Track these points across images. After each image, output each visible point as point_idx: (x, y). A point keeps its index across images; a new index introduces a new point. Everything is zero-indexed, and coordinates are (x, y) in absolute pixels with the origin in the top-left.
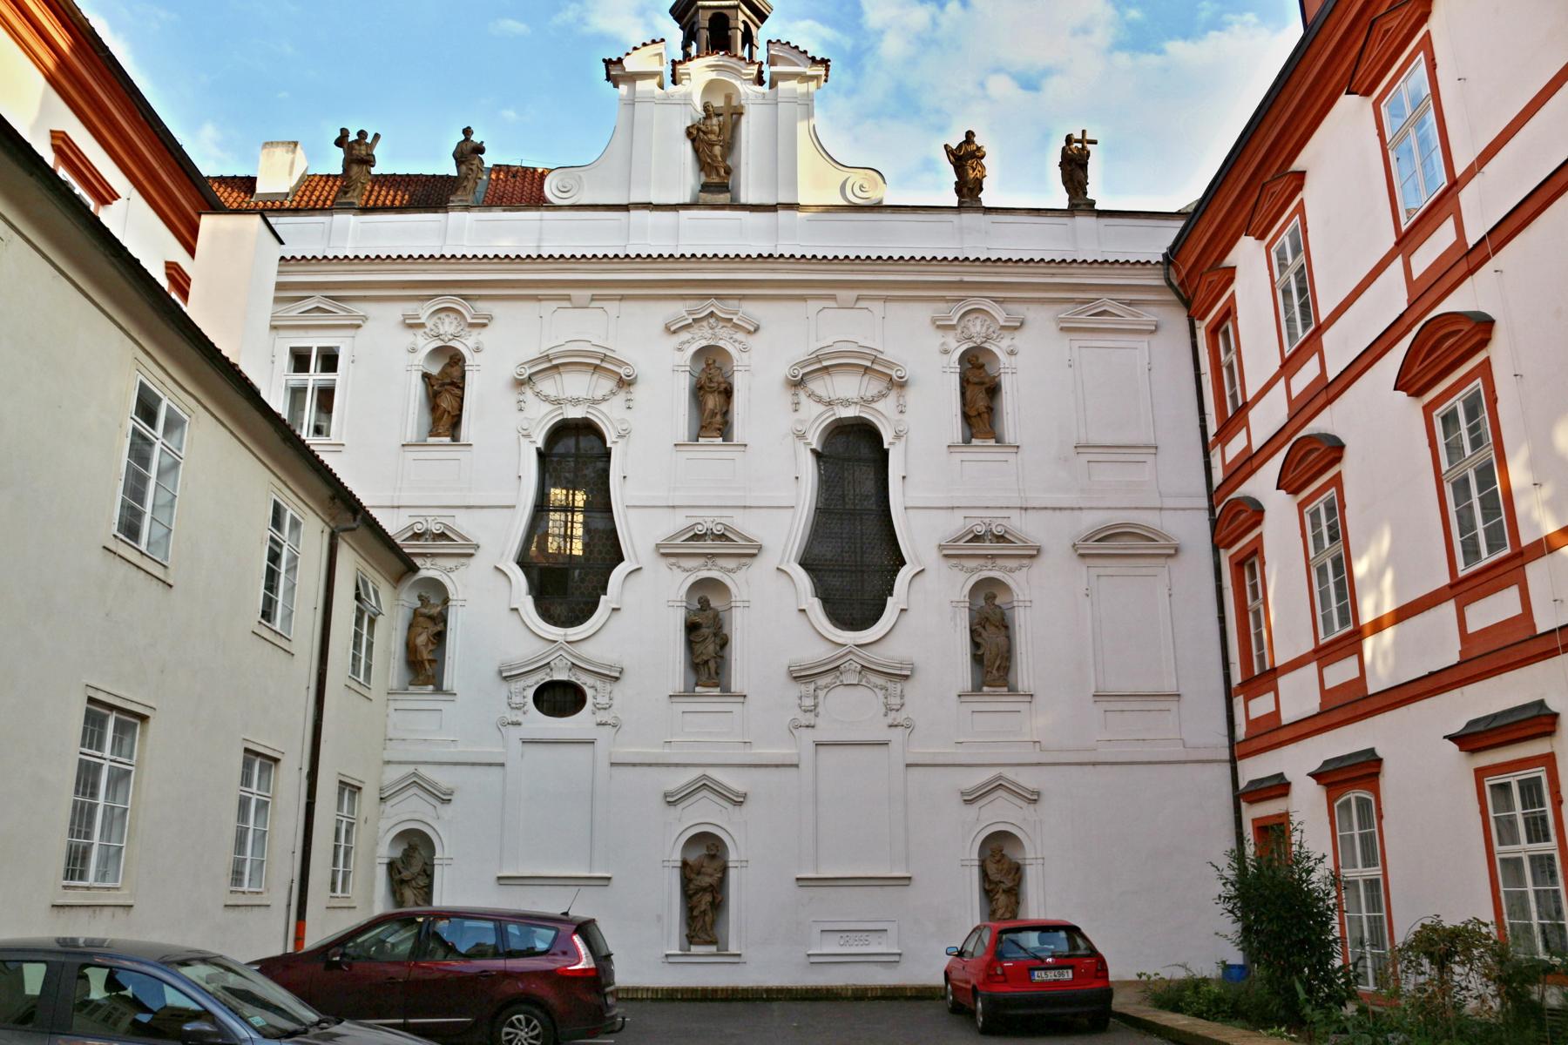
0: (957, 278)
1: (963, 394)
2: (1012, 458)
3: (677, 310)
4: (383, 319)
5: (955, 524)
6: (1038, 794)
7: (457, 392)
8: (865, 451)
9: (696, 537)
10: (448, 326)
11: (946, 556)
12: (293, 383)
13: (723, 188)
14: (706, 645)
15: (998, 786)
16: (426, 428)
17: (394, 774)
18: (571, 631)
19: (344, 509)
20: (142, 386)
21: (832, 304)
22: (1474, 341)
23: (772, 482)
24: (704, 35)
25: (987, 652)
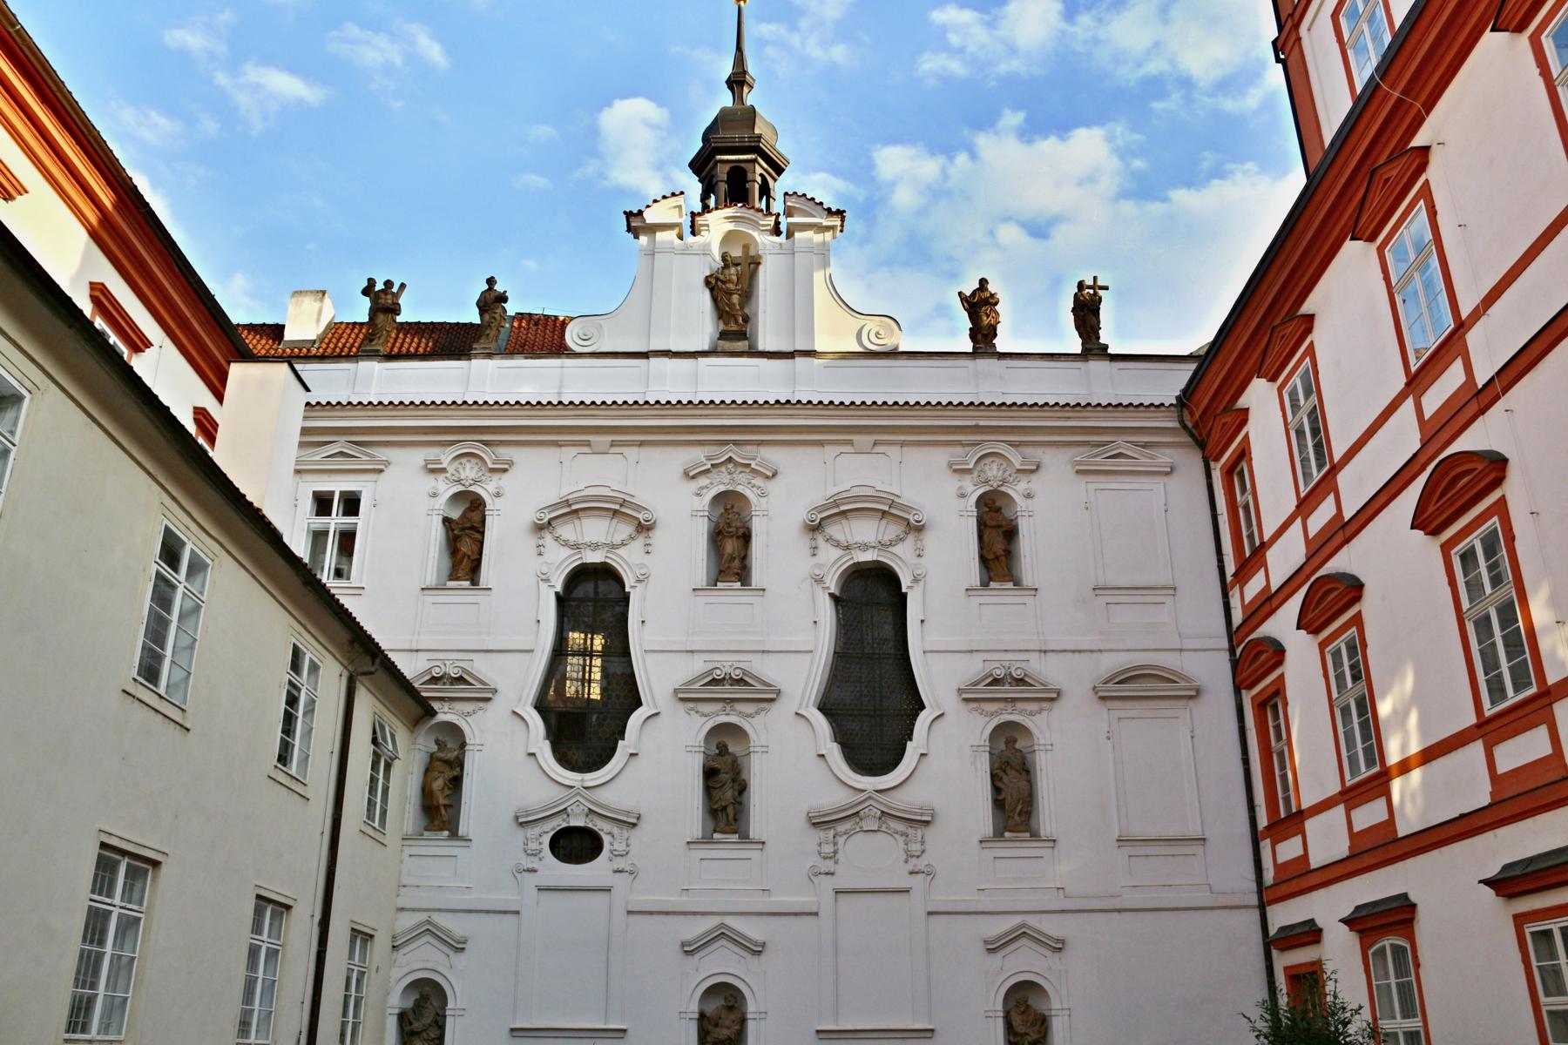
0: (972, 423)
1: (980, 537)
2: (1029, 600)
3: (697, 455)
4: (406, 464)
5: (975, 668)
6: (1063, 942)
7: (478, 536)
8: (883, 594)
9: (714, 682)
10: (469, 471)
11: (966, 700)
12: (313, 527)
13: (741, 335)
14: (725, 791)
15: (1021, 934)
17: (407, 921)
19: (363, 654)
20: (167, 531)
22: (1487, 480)
23: (790, 628)
24: (723, 187)
25: (1009, 796)
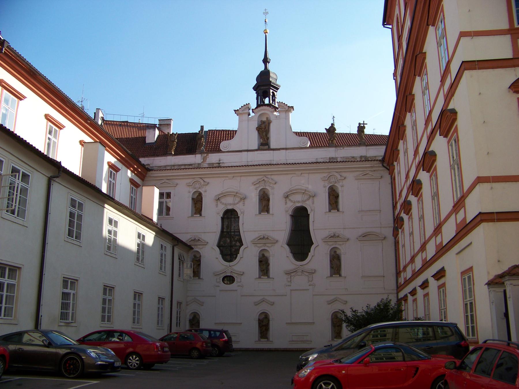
1: (329, 197)
3: (255, 179)
5: (326, 233)
14: (264, 264)
16: (194, 211)
21: (294, 175)
23: (279, 224)
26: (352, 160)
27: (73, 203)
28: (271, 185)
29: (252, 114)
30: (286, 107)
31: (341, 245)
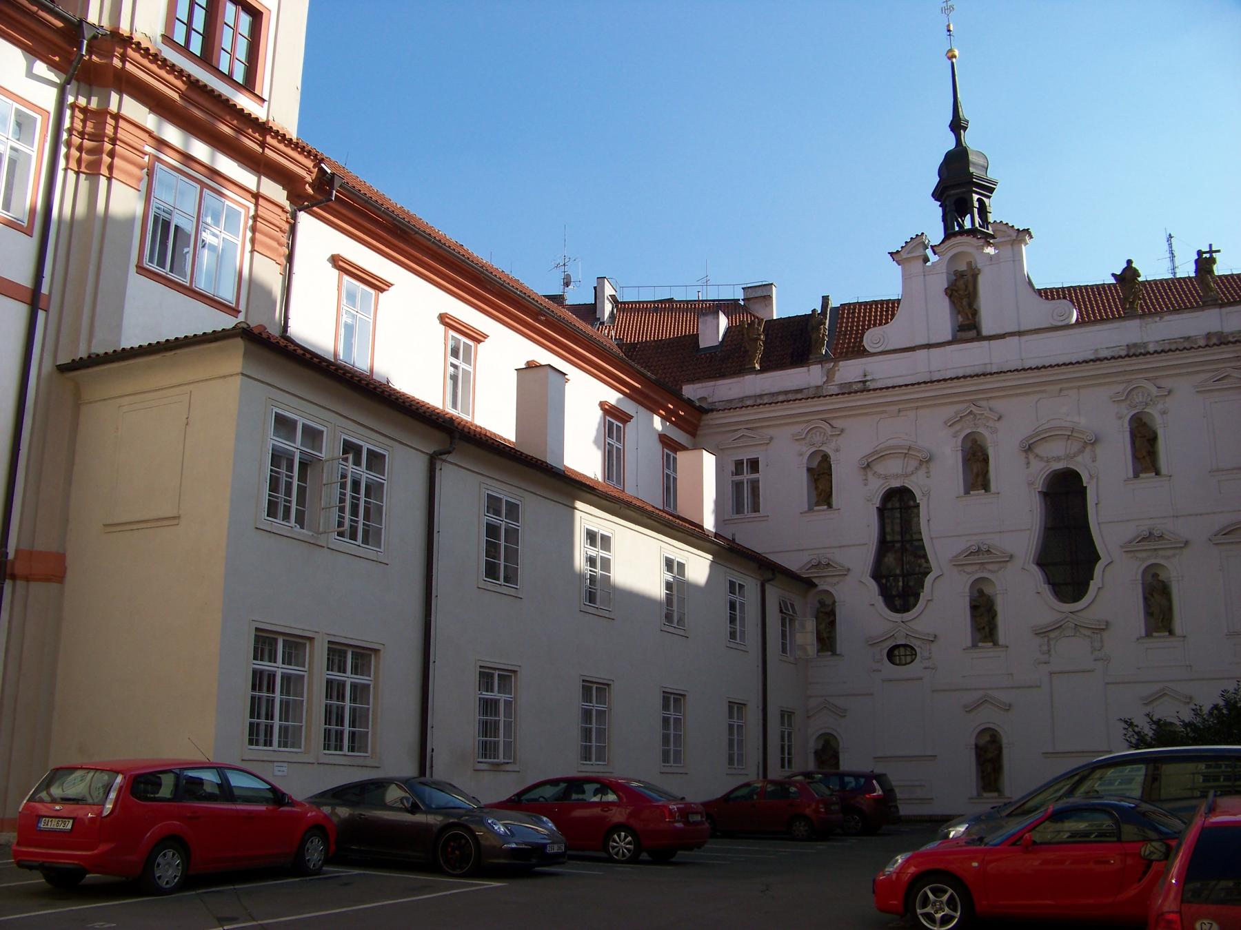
1: (1133, 443)
3: (950, 411)
14: (983, 613)
18: (905, 615)
26: (1186, 345)
27: (493, 504)
28: (990, 424)
29: (933, 258)
30: (1010, 232)
31: (1168, 558)
